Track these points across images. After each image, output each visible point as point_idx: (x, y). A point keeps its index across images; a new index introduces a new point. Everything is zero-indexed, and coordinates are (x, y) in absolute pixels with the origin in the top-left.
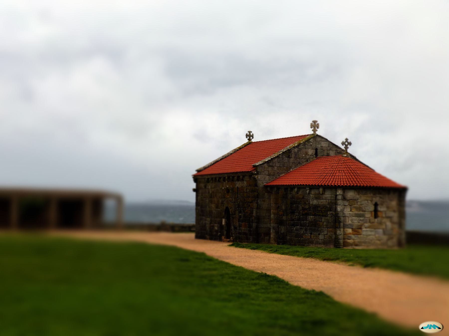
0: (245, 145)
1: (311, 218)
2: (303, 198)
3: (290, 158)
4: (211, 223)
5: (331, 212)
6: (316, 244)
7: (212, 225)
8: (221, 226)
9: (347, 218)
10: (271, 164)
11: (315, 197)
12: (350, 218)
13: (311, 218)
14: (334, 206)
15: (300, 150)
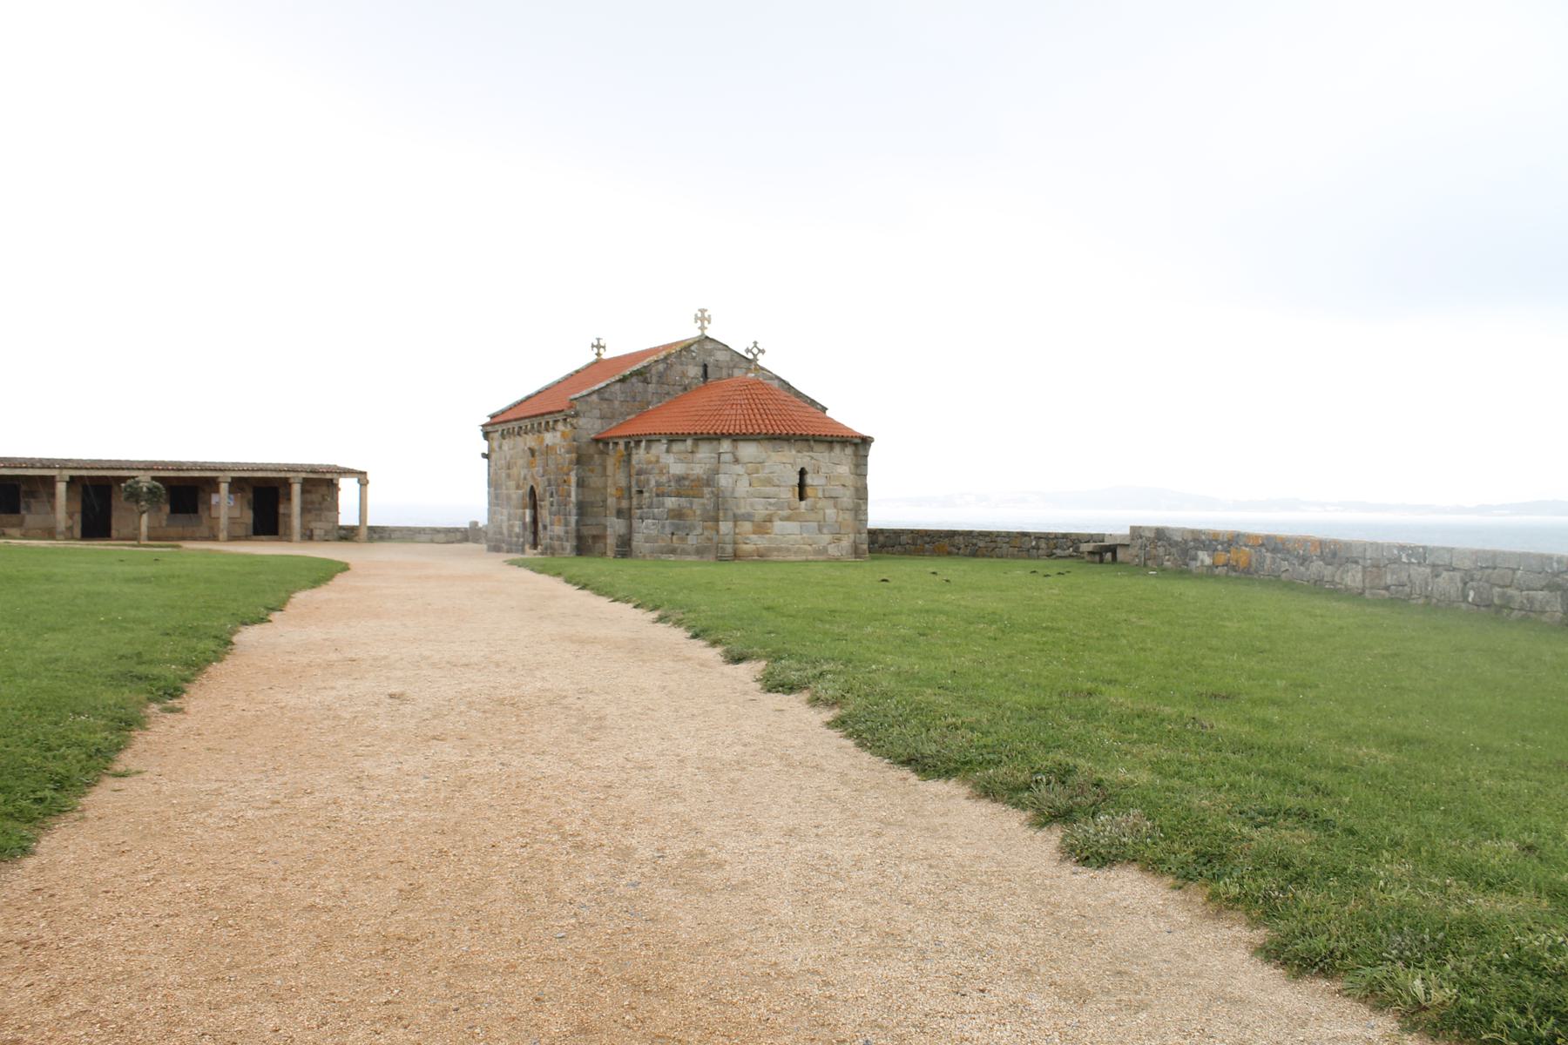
2: (657, 462)
3: (648, 383)
4: (509, 520)
5: (710, 489)
6: (681, 554)
7: (511, 522)
8: (524, 524)
9: (742, 500)
10: (606, 396)
11: (679, 459)
12: (749, 500)
13: (670, 502)
15: (669, 367)
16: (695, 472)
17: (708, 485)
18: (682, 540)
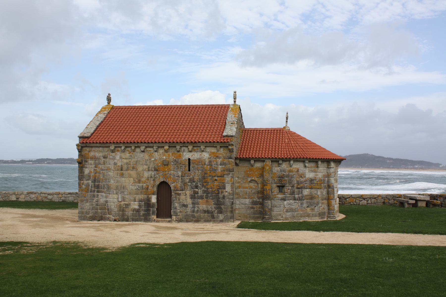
11: (311, 170)
13: (306, 192)
14: (326, 179)
16: (318, 177)
17: (324, 183)
18: (313, 210)
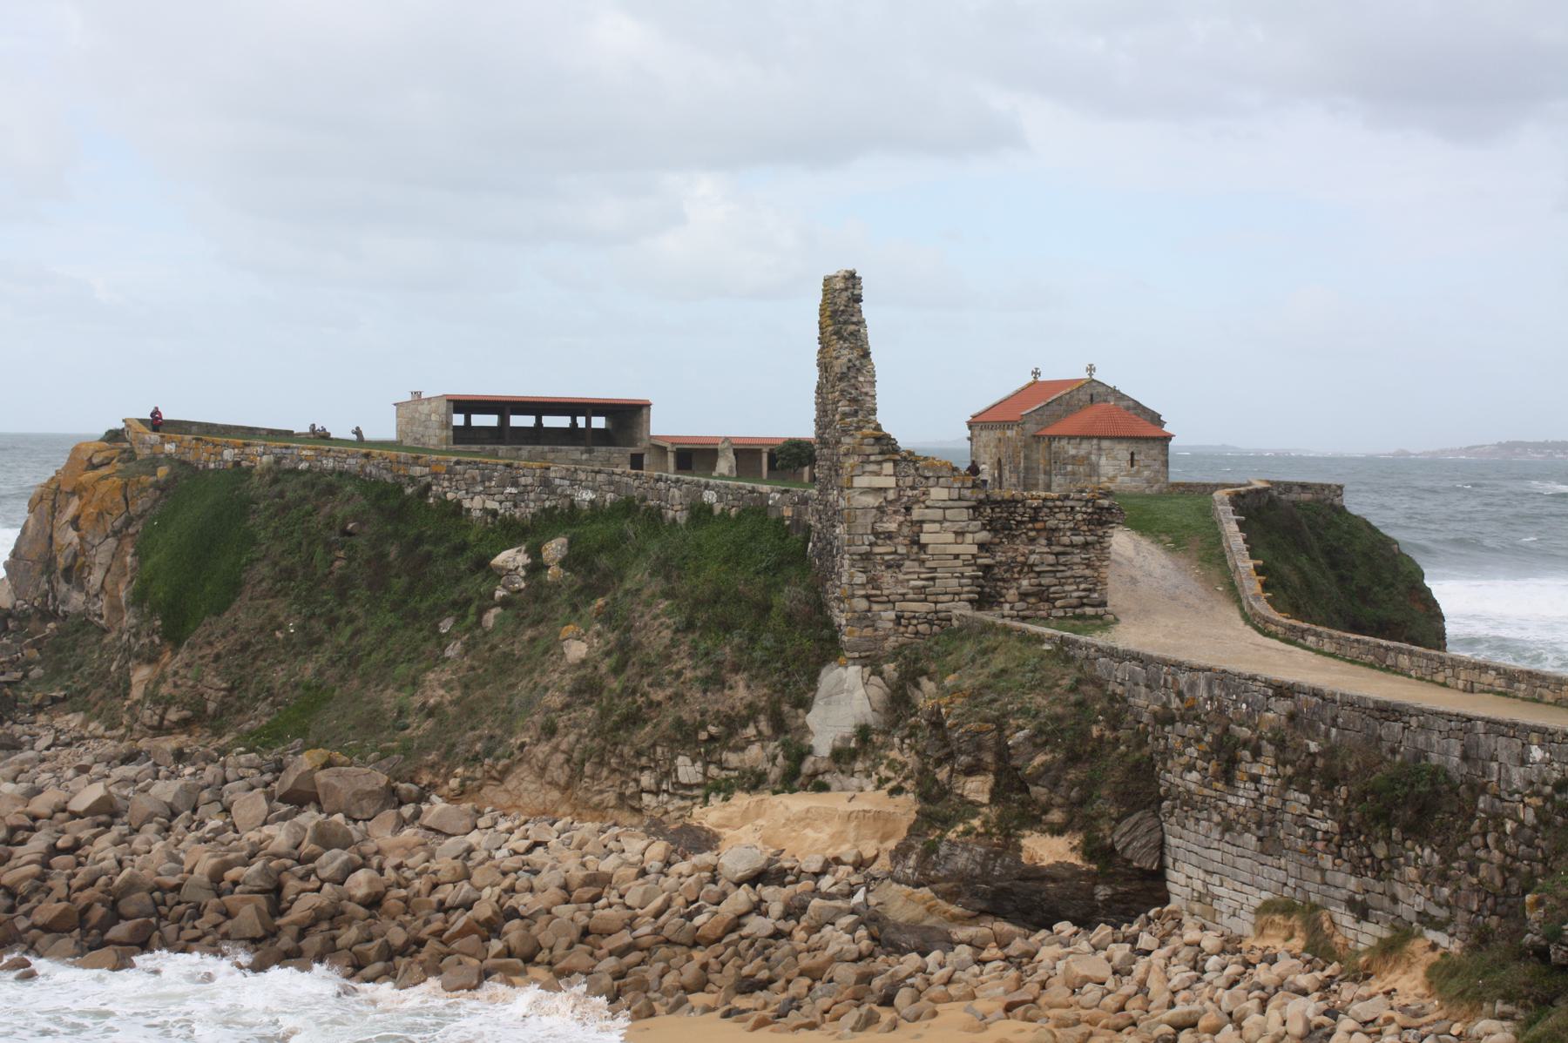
0: (1030, 385)
1: (1069, 468)
13: (1069, 468)
15: (1072, 397)
